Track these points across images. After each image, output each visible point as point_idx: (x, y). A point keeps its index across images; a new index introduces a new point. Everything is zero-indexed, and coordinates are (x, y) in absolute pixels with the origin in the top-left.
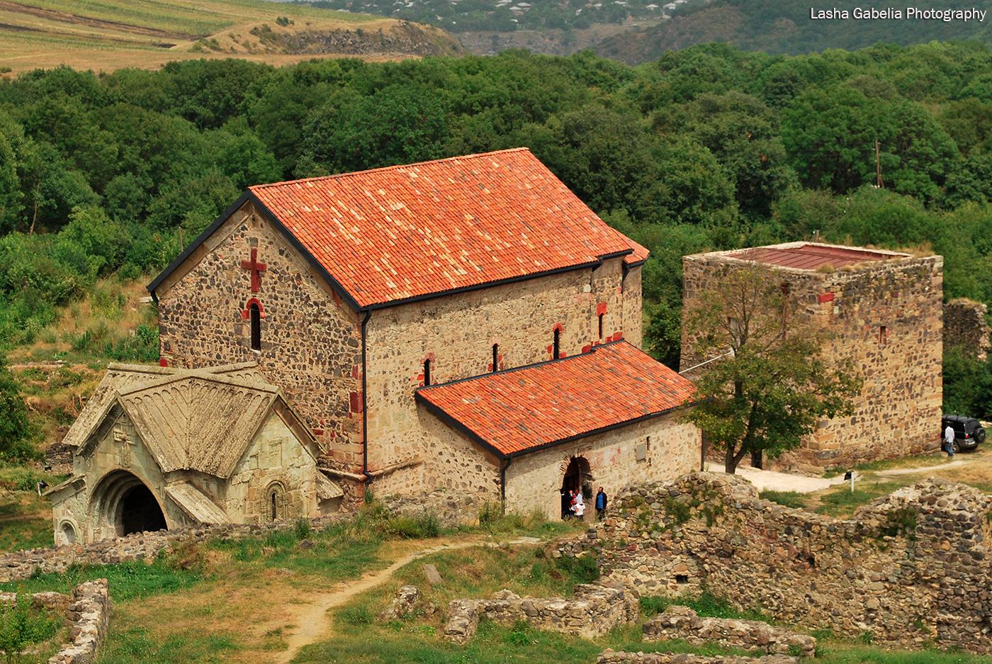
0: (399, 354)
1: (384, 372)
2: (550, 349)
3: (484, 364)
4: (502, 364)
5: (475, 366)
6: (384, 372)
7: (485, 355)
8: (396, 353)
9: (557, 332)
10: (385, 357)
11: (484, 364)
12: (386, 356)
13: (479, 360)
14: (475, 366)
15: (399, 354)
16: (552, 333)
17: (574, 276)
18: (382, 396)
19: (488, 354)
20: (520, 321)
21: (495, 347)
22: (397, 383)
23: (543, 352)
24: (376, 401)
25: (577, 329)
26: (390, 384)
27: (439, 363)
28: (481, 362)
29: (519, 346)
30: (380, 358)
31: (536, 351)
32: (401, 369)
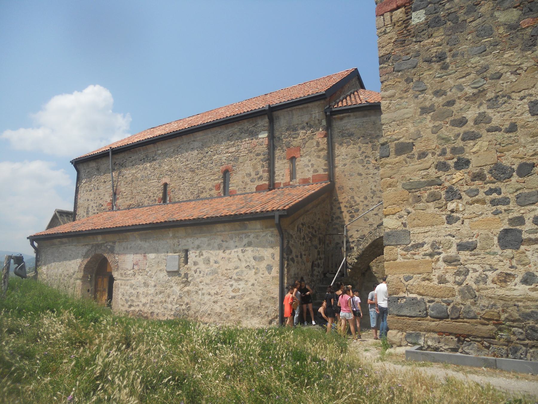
0: (98, 189)
1: (88, 200)
2: (218, 187)
3: (155, 198)
4: (170, 198)
5: (147, 199)
6: (88, 200)
7: (156, 191)
8: (96, 189)
9: (226, 174)
10: (90, 191)
11: (155, 198)
12: (91, 191)
13: (151, 194)
14: (147, 199)
15: (98, 189)
16: (221, 174)
17: (246, 125)
18: (85, 214)
19: (158, 190)
20: (188, 166)
21: (166, 185)
22: (94, 208)
23: (211, 190)
24: (82, 217)
25: (250, 170)
26: (90, 207)
27: (122, 196)
28: (152, 196)
29: (186, 184)
30: (87, 191)
31: (204, 188)
32: (98, 198)
